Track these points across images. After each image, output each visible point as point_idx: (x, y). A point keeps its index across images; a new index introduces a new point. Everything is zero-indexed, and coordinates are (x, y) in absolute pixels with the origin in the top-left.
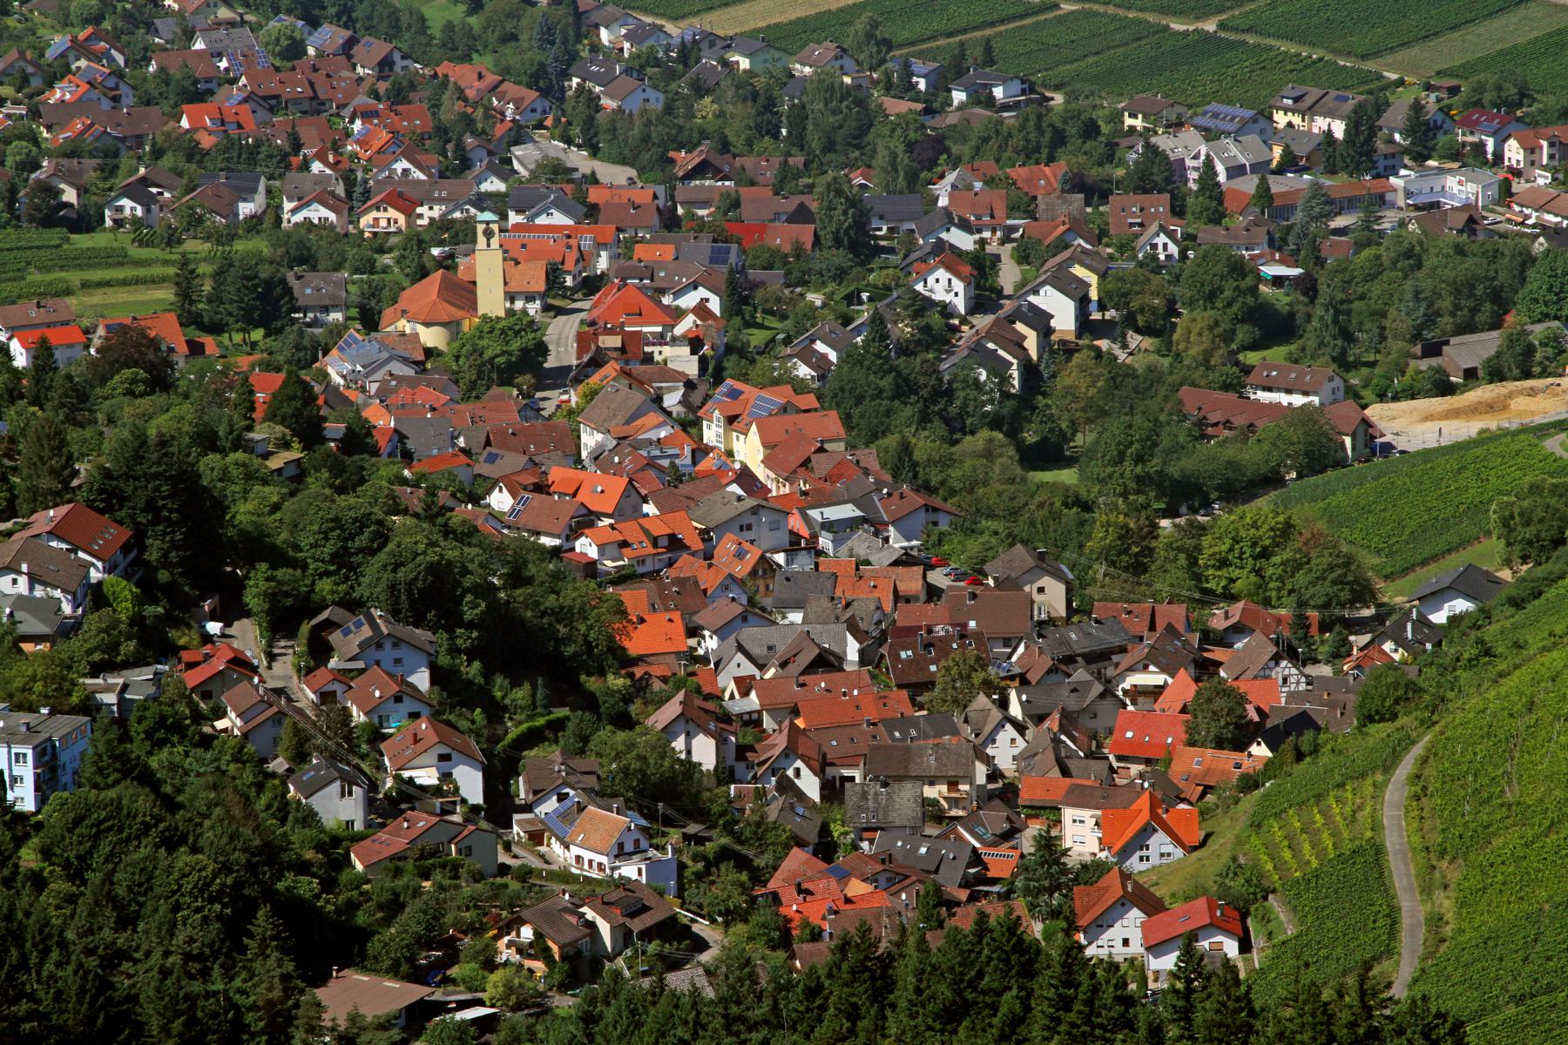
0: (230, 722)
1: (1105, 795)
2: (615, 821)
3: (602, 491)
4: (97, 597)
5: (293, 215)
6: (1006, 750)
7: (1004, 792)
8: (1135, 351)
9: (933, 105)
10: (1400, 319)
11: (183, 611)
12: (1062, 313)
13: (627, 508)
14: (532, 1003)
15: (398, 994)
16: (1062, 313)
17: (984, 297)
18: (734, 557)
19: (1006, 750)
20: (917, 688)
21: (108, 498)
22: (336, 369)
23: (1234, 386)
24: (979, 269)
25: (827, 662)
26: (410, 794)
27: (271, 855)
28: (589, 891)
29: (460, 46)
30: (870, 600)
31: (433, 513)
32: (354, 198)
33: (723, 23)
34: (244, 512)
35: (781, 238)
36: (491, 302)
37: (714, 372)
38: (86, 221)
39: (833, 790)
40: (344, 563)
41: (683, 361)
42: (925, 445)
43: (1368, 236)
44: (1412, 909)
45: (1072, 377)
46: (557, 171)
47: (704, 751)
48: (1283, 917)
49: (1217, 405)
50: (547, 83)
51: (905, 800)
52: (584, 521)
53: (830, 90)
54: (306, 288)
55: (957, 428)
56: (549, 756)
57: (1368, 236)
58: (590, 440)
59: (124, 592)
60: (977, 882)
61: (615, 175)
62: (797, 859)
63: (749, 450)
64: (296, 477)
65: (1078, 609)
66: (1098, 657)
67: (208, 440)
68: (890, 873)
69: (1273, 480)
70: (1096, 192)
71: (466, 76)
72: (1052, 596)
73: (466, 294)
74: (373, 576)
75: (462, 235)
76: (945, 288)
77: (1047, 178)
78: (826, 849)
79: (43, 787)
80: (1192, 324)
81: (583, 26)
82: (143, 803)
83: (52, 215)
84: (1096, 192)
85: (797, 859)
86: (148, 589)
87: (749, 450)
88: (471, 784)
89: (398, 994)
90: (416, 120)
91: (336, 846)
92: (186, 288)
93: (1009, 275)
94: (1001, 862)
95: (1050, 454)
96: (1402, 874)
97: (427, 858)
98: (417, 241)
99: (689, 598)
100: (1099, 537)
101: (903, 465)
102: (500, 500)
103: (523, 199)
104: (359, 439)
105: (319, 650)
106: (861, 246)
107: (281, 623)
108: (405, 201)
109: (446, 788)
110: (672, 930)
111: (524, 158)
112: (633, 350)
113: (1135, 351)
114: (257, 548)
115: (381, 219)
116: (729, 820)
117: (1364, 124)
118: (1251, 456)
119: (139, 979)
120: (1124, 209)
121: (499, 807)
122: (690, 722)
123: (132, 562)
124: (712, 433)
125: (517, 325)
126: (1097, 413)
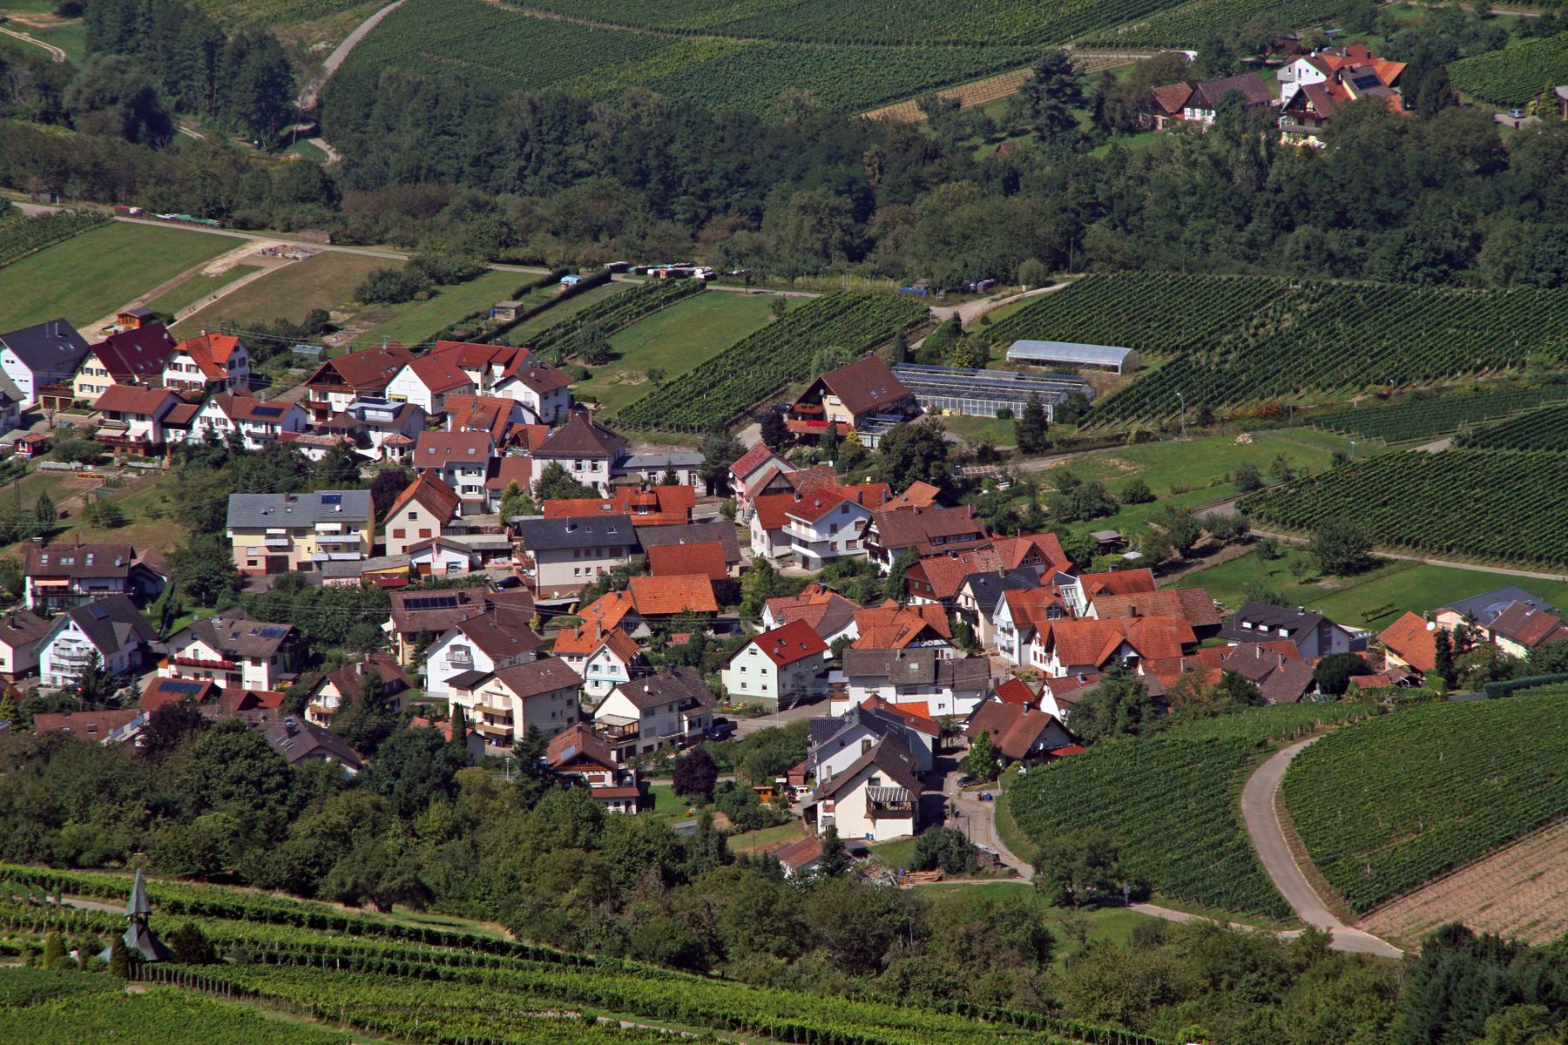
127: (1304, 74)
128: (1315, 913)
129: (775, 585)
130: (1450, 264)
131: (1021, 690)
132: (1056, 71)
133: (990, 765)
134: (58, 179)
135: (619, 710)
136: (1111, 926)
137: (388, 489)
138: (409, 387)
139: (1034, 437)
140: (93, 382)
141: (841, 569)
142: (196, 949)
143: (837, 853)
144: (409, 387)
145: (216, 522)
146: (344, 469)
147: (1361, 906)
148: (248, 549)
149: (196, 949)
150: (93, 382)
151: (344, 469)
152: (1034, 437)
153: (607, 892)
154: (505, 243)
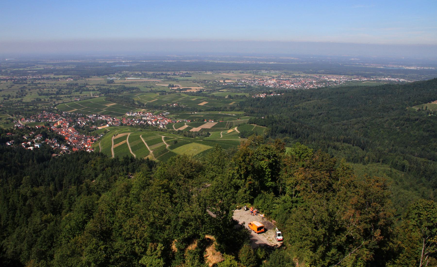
0: (48, 143)
1: (87, 144)
2: (65, 147)
3: (64, 132)
4: (41, 138)
5: (50, 121)
6: (83, 143)
7: (83, 144)
8: (87, 125)
9: (78, 115)
10: (99, 123)
11: (46, 139)
12: (84, 124)
13: (65, 133)
14: (62, 154)
15: (55, 155)
16: (84, 124)
17: (81, 123)
18: (70, 135)
19: (83, 143)
20: (79, 140)
21: (42, 134)
22: (52, 128)
23: (92, 126)
24: (80, 122)
25: (75, 139)
26: (56, 146)
27: (50, 149)
28: (65, 150)
29: (57, 113)
30: (77, 136)
31: (56, 134)
32: (52, 120)
33: (69, 112)
34: (48, 134)
35: (72, 121)
36: (59, 124)
37: (69, 127)
38: (40, 122)
39: (75, 145)
40: (53, 136)
41: (68, 127)
42: (78, 130)
43: (97, 120)
44: (100, 148)
45: (85, 126)
46: (61, 119)
47: (69, 143)
48: (95, 149)
49: (90, 127)
50: (61, 115)
51: (78, 145)
52: (63, 134)
53: (73, 115)
54: (50, 124)
55: (80, 129)
56: (62, 144)
57: (97, 120)
58: (63, 130)
59: (43, 138)
60: (82, 148)
61: (64, 119)
62: (74, 148)
63: (71, 130)
64: (50, 132)
65: (86, 136)
66: (87, 138)
67: (46, 131)
68: (78, 148)
69: (94, 130)
70: (85, 119)
71: (57, 115)
72: (84, 136)
73: (57, 124)
74: (54, 136)
75: (57, 121)
76: (79, 123)
77: (83, 118)
78: (75, 147)
79: (40, 146)
80: (90, 124)
81: (62, 112)
82: (44, 147)
83: (39, 121)
84: (85, 119)
85: (74, 148)
86: (44, 138)
87: (71, 130)
88: (59, 145)
89: (55, 155)
90: (55, 117)
91: (53, 148)
92: (45, 124)
93: (82, 122)
94: (83, 147)
95: (84, 130)
96: (100, 147)
97: (57, 149)
98: (55, 122)
99: (68, 137)
100: (86, 133)
101: (77, 131)
102: (59, 133)
103: (60, 120)
104: (53, 130)
105: (52, 140)
106: (75, 121)
107: (50, 139)
108: (55, 120)
109: (58, 146)
110: (68, 151)
111: (60, 118)
112: (65, 126)
113: (87, 125)
114: (49, 136)
115: (54, 121)
116: (71, 146)
117: (97, 115)
118: (93, 129)
119: (44, 155)
120: (87, 119)
121: (60, 146)
122: (69, 142)
123: (43, 136)
124: (69, 130)
125: (60, 125)
126: (86, 128)
127: (174, 105)
128: (175, 129)
129: (159, 120)
130: (179, 110)
131: (166, 123)
132: (167, 105)
133: (165, 125)
134: (137, 107)
135: (154, 123)
136: (169, 130)
137: (147, 117)
138: (148, 114)
139: (167, 115)
140: (138, 114)
141: (161, 119)
142: (141, 131)
143: (161, 128)
144: (148, 114)
145: (142, 118)
146: (146, 116)
147: (176, 129)
148: (143, 119)
149: (141, 131)
150: (138, 114)
151: (146, 116)
152: (167, 115)
153: (154, 129)
154: (151, 109)
